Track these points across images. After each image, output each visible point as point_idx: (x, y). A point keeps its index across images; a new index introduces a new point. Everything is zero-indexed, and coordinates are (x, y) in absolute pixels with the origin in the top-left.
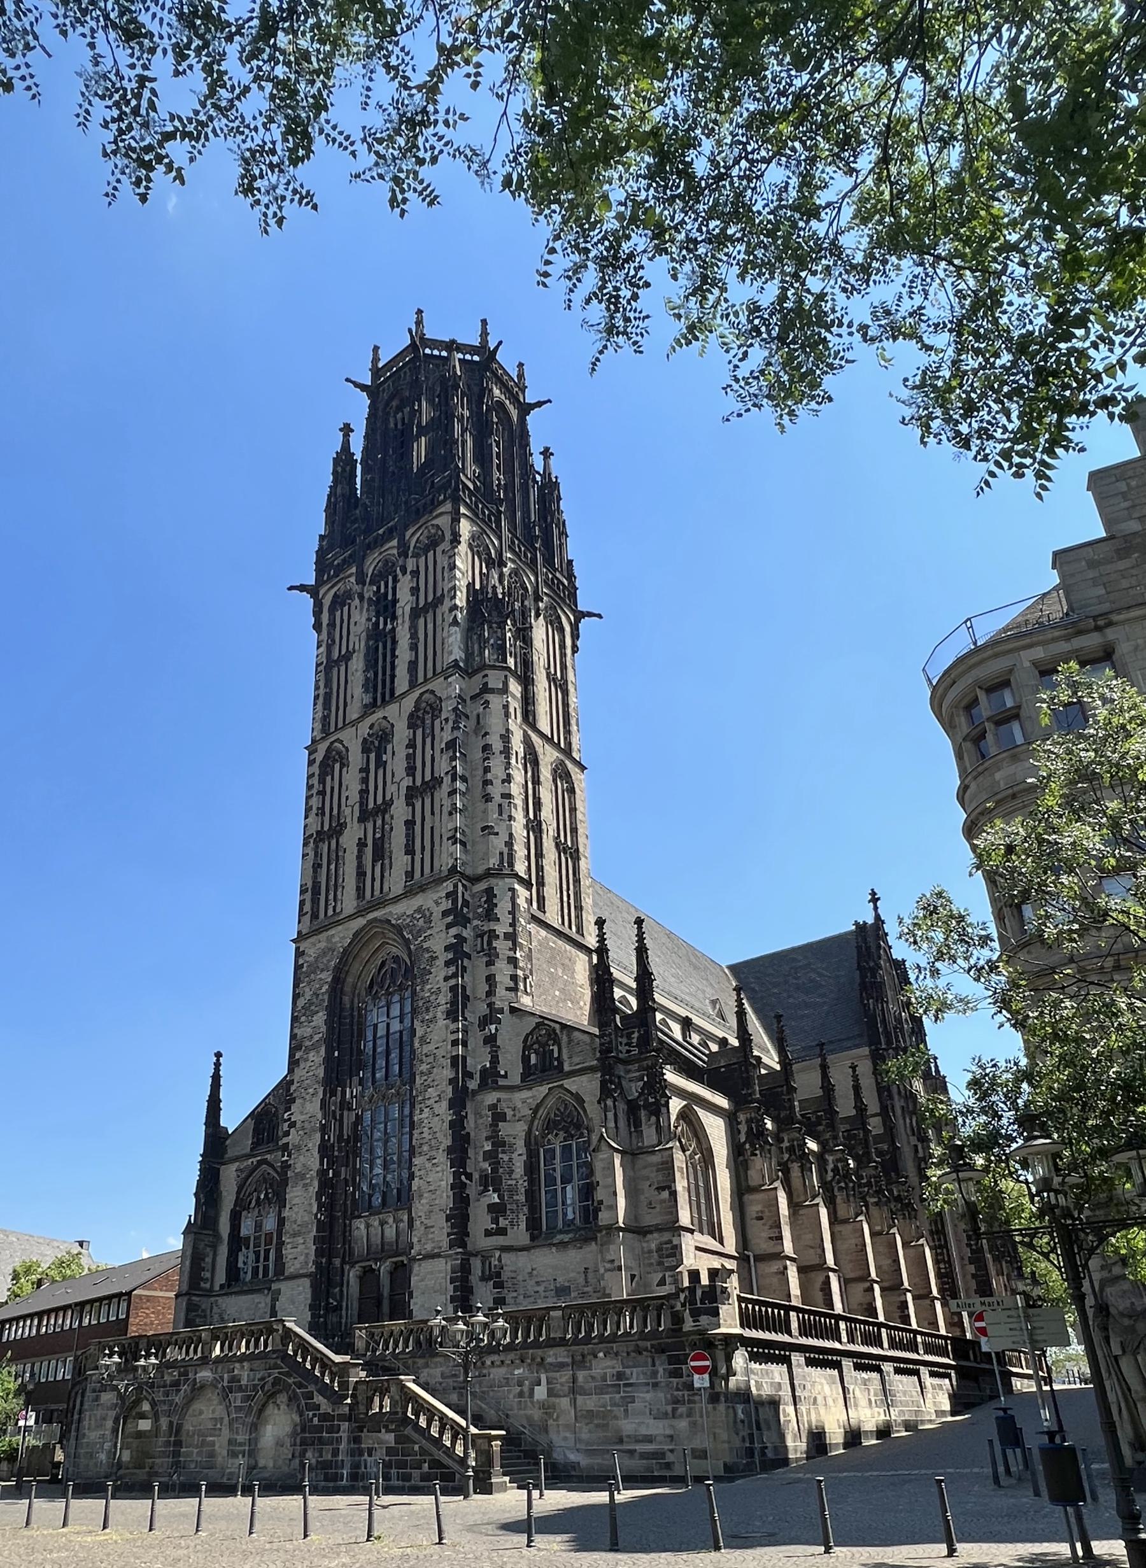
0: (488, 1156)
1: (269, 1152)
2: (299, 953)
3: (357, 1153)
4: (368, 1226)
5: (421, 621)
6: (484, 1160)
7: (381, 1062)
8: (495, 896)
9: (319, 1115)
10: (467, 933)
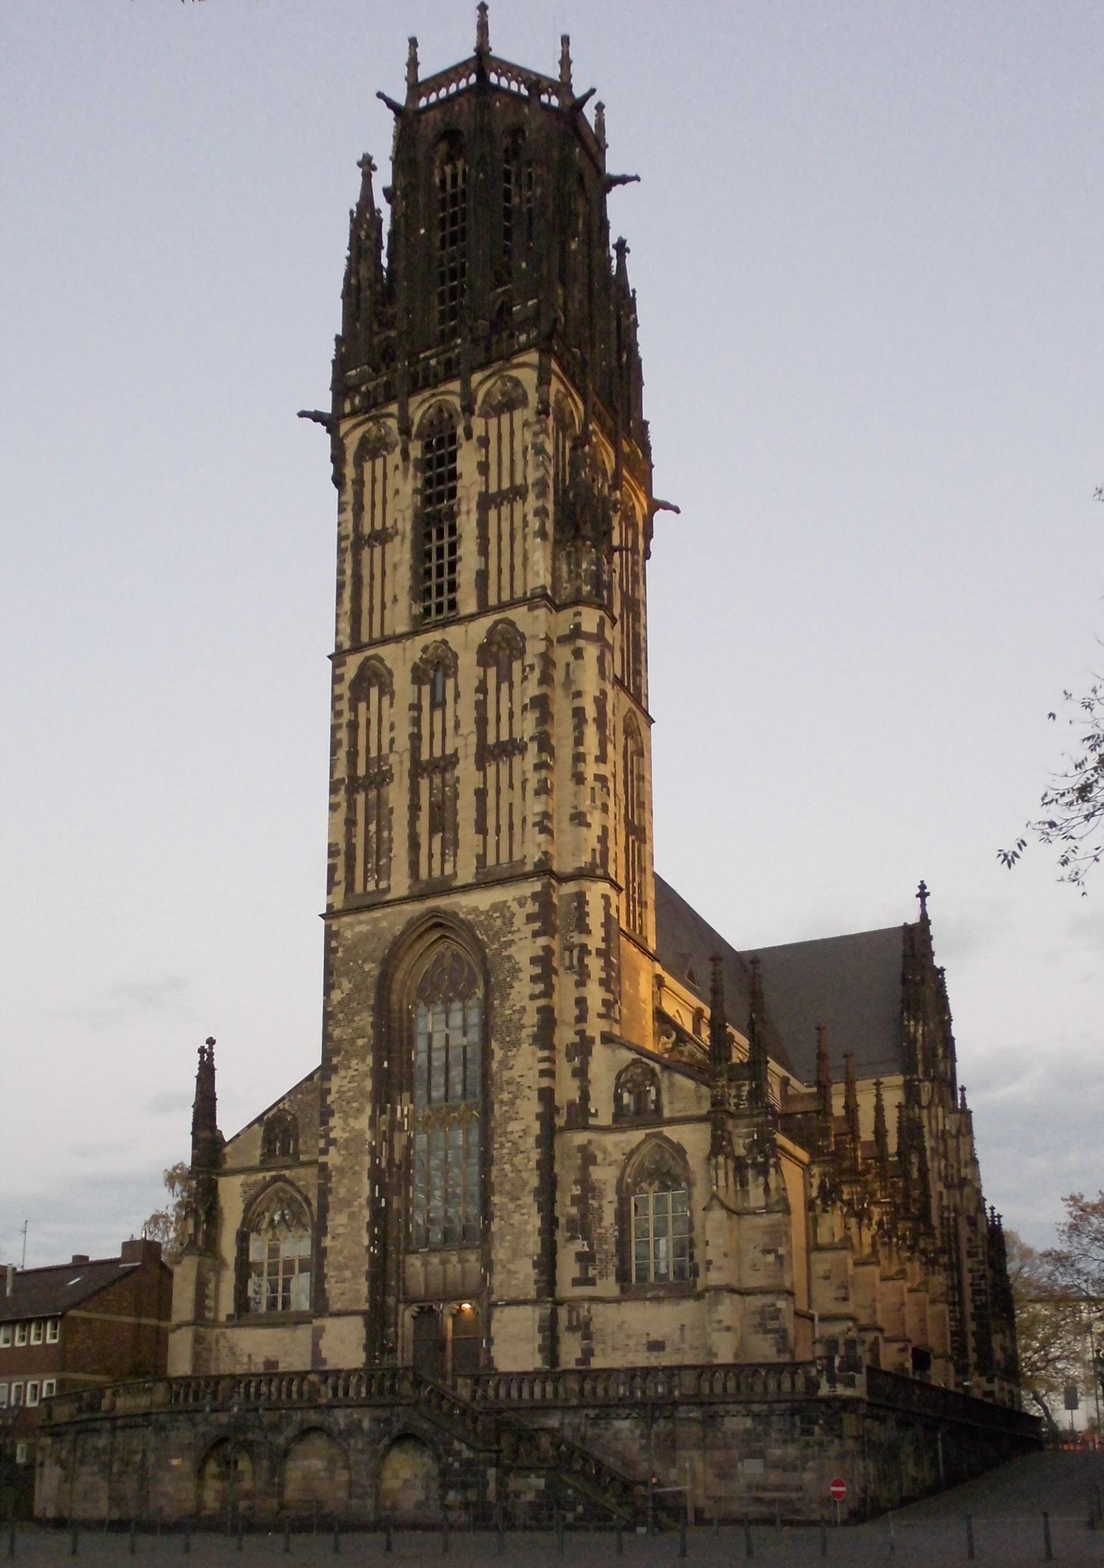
0: (575, 1200)
1: (287, 1167)
2: (330, 935)
3: (409, 1181)
4: (426, 1264)
6: (573, 1204)
7: (438, 1079)
8: (587, 903)
9: (368, 1135)
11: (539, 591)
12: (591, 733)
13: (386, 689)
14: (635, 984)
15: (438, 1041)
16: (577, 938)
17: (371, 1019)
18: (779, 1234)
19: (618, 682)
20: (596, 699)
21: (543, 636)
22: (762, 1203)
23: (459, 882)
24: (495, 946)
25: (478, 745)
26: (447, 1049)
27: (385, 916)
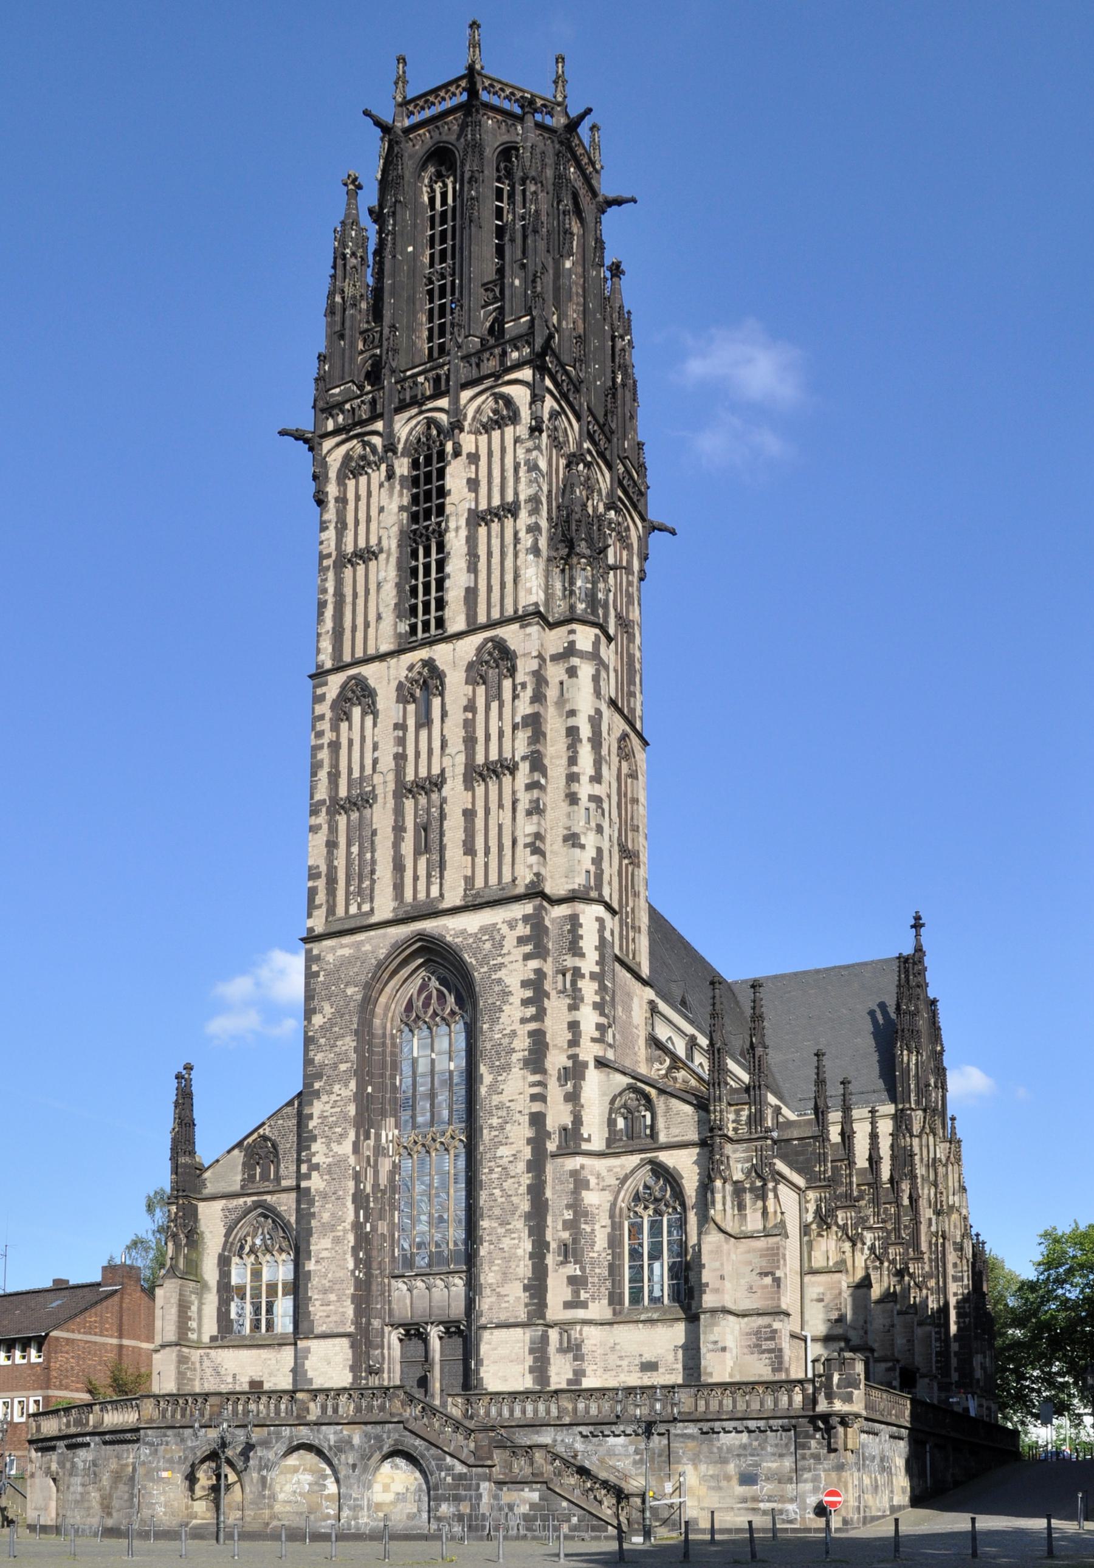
0: (568, 1225)
6: (564, 1230)
8: (581, 926)
9: (352, 1160)
11: (531, 609)
13: (371, 709)
14: (628, 1010)
15: (423, 1067)
16: (570, 962)
17: (354, 1044)
18: (775, 1256)
19: (613, 703)
20: (591, 719)
21: (535, 654)
22: (761, 1227)
23: (446, 904)
24: (485, 969)
25: (466, 765)
26: (433, 1072)
27: (369, 940)
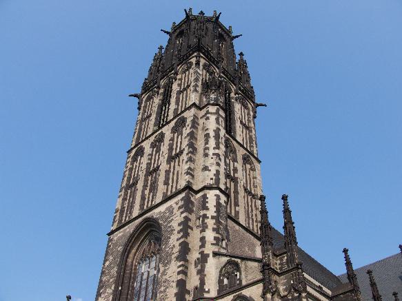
5: (181, 95)
7: (143, 293)
10: (193, 217)
12: (212, 143)
16: (202, 213)
